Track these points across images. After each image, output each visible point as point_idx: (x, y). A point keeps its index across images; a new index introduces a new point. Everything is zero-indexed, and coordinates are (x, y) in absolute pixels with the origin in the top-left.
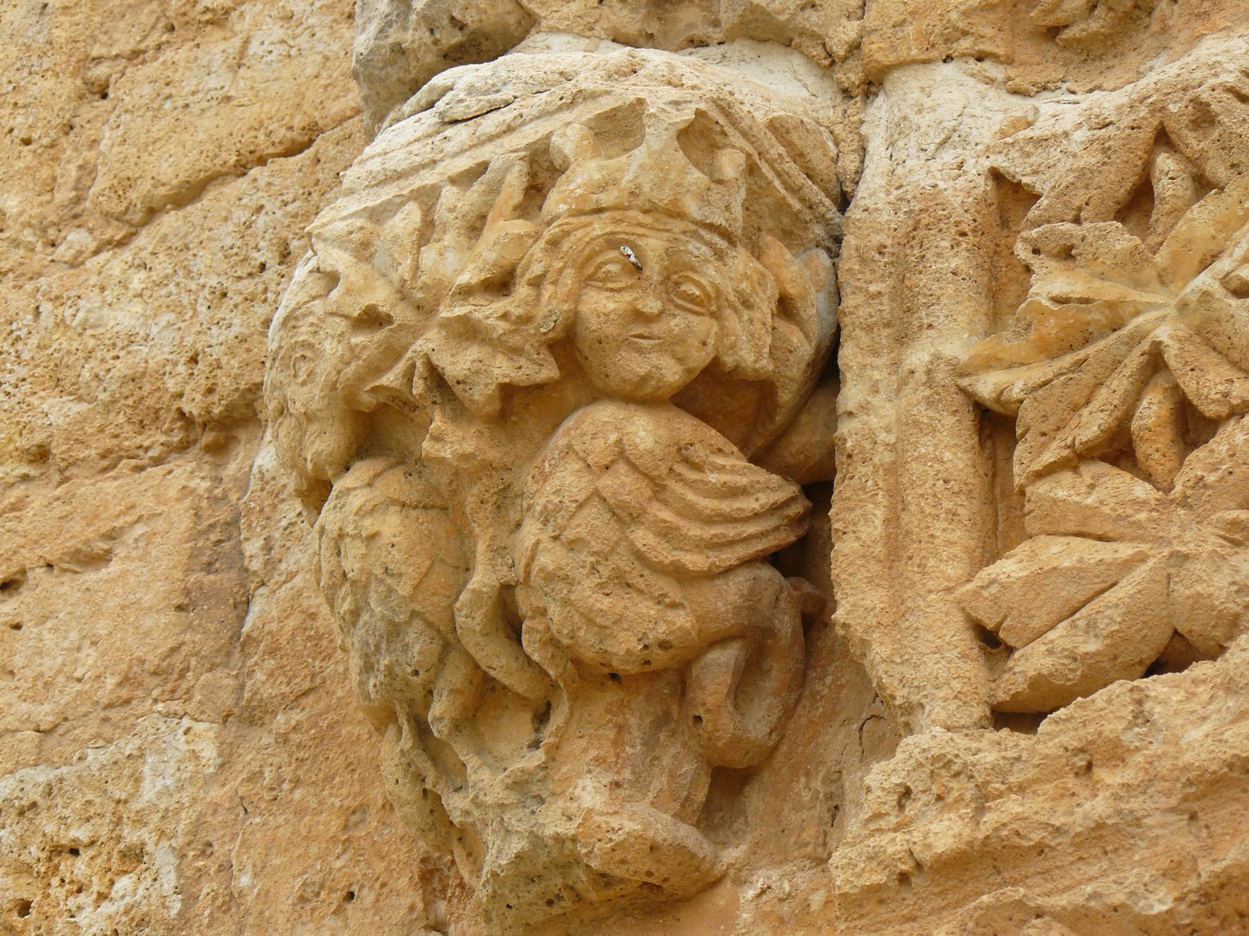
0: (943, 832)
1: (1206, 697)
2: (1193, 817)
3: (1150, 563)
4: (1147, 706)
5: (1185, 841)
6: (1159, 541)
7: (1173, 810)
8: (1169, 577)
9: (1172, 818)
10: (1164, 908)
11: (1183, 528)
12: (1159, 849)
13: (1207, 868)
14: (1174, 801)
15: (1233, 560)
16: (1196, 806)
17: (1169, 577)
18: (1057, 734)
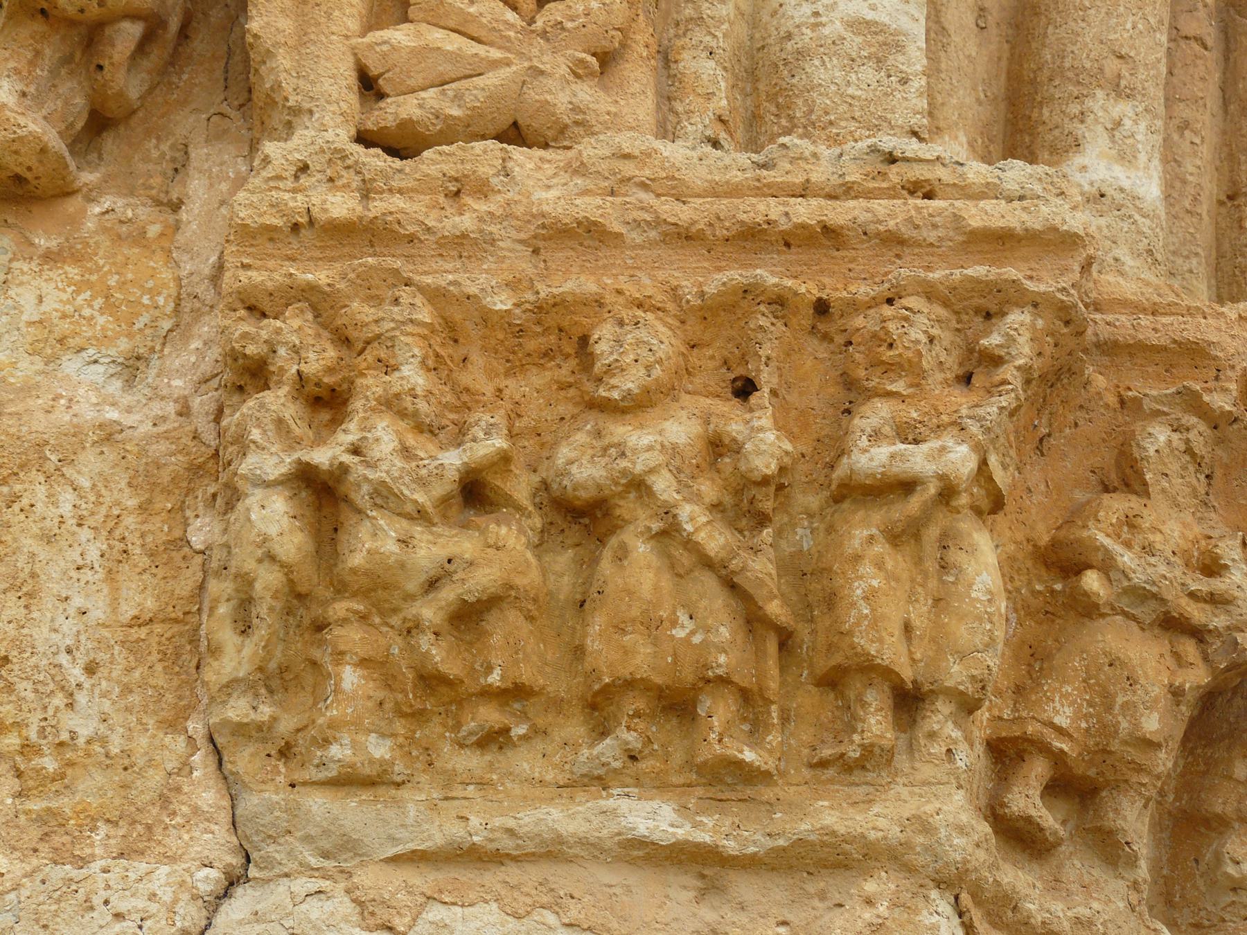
0: (340, 205)
1: (550, 172)
2: (536, 251)
3: (514, 68)
4: (510, 164)
5: (526, 266)
6: (521, 55)
7: (521, 242)
8: (524, 82)
9: (519, 247)
10: (505, 308)
11: (542, 52)
12: (504, 266)
13: (544, 291)
14: (523, 236)
15: (573, 86)
16: (541, 244)
17: (524, 82)
18: (433, 162)
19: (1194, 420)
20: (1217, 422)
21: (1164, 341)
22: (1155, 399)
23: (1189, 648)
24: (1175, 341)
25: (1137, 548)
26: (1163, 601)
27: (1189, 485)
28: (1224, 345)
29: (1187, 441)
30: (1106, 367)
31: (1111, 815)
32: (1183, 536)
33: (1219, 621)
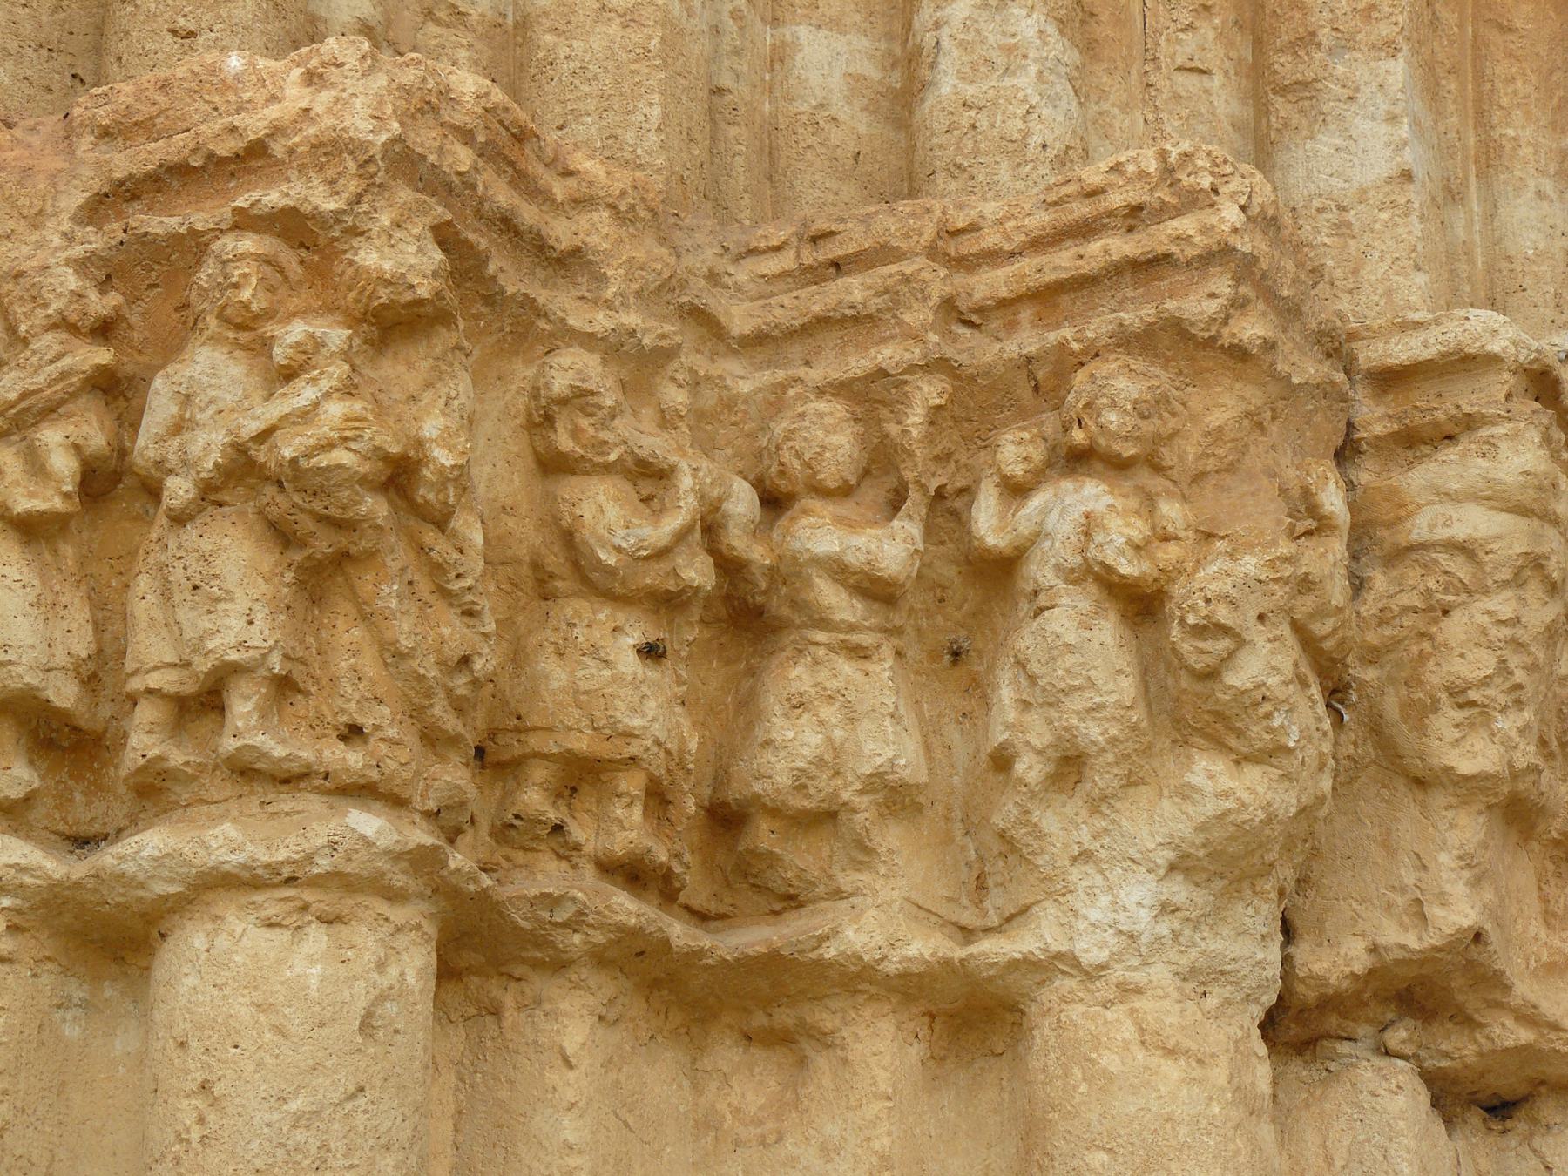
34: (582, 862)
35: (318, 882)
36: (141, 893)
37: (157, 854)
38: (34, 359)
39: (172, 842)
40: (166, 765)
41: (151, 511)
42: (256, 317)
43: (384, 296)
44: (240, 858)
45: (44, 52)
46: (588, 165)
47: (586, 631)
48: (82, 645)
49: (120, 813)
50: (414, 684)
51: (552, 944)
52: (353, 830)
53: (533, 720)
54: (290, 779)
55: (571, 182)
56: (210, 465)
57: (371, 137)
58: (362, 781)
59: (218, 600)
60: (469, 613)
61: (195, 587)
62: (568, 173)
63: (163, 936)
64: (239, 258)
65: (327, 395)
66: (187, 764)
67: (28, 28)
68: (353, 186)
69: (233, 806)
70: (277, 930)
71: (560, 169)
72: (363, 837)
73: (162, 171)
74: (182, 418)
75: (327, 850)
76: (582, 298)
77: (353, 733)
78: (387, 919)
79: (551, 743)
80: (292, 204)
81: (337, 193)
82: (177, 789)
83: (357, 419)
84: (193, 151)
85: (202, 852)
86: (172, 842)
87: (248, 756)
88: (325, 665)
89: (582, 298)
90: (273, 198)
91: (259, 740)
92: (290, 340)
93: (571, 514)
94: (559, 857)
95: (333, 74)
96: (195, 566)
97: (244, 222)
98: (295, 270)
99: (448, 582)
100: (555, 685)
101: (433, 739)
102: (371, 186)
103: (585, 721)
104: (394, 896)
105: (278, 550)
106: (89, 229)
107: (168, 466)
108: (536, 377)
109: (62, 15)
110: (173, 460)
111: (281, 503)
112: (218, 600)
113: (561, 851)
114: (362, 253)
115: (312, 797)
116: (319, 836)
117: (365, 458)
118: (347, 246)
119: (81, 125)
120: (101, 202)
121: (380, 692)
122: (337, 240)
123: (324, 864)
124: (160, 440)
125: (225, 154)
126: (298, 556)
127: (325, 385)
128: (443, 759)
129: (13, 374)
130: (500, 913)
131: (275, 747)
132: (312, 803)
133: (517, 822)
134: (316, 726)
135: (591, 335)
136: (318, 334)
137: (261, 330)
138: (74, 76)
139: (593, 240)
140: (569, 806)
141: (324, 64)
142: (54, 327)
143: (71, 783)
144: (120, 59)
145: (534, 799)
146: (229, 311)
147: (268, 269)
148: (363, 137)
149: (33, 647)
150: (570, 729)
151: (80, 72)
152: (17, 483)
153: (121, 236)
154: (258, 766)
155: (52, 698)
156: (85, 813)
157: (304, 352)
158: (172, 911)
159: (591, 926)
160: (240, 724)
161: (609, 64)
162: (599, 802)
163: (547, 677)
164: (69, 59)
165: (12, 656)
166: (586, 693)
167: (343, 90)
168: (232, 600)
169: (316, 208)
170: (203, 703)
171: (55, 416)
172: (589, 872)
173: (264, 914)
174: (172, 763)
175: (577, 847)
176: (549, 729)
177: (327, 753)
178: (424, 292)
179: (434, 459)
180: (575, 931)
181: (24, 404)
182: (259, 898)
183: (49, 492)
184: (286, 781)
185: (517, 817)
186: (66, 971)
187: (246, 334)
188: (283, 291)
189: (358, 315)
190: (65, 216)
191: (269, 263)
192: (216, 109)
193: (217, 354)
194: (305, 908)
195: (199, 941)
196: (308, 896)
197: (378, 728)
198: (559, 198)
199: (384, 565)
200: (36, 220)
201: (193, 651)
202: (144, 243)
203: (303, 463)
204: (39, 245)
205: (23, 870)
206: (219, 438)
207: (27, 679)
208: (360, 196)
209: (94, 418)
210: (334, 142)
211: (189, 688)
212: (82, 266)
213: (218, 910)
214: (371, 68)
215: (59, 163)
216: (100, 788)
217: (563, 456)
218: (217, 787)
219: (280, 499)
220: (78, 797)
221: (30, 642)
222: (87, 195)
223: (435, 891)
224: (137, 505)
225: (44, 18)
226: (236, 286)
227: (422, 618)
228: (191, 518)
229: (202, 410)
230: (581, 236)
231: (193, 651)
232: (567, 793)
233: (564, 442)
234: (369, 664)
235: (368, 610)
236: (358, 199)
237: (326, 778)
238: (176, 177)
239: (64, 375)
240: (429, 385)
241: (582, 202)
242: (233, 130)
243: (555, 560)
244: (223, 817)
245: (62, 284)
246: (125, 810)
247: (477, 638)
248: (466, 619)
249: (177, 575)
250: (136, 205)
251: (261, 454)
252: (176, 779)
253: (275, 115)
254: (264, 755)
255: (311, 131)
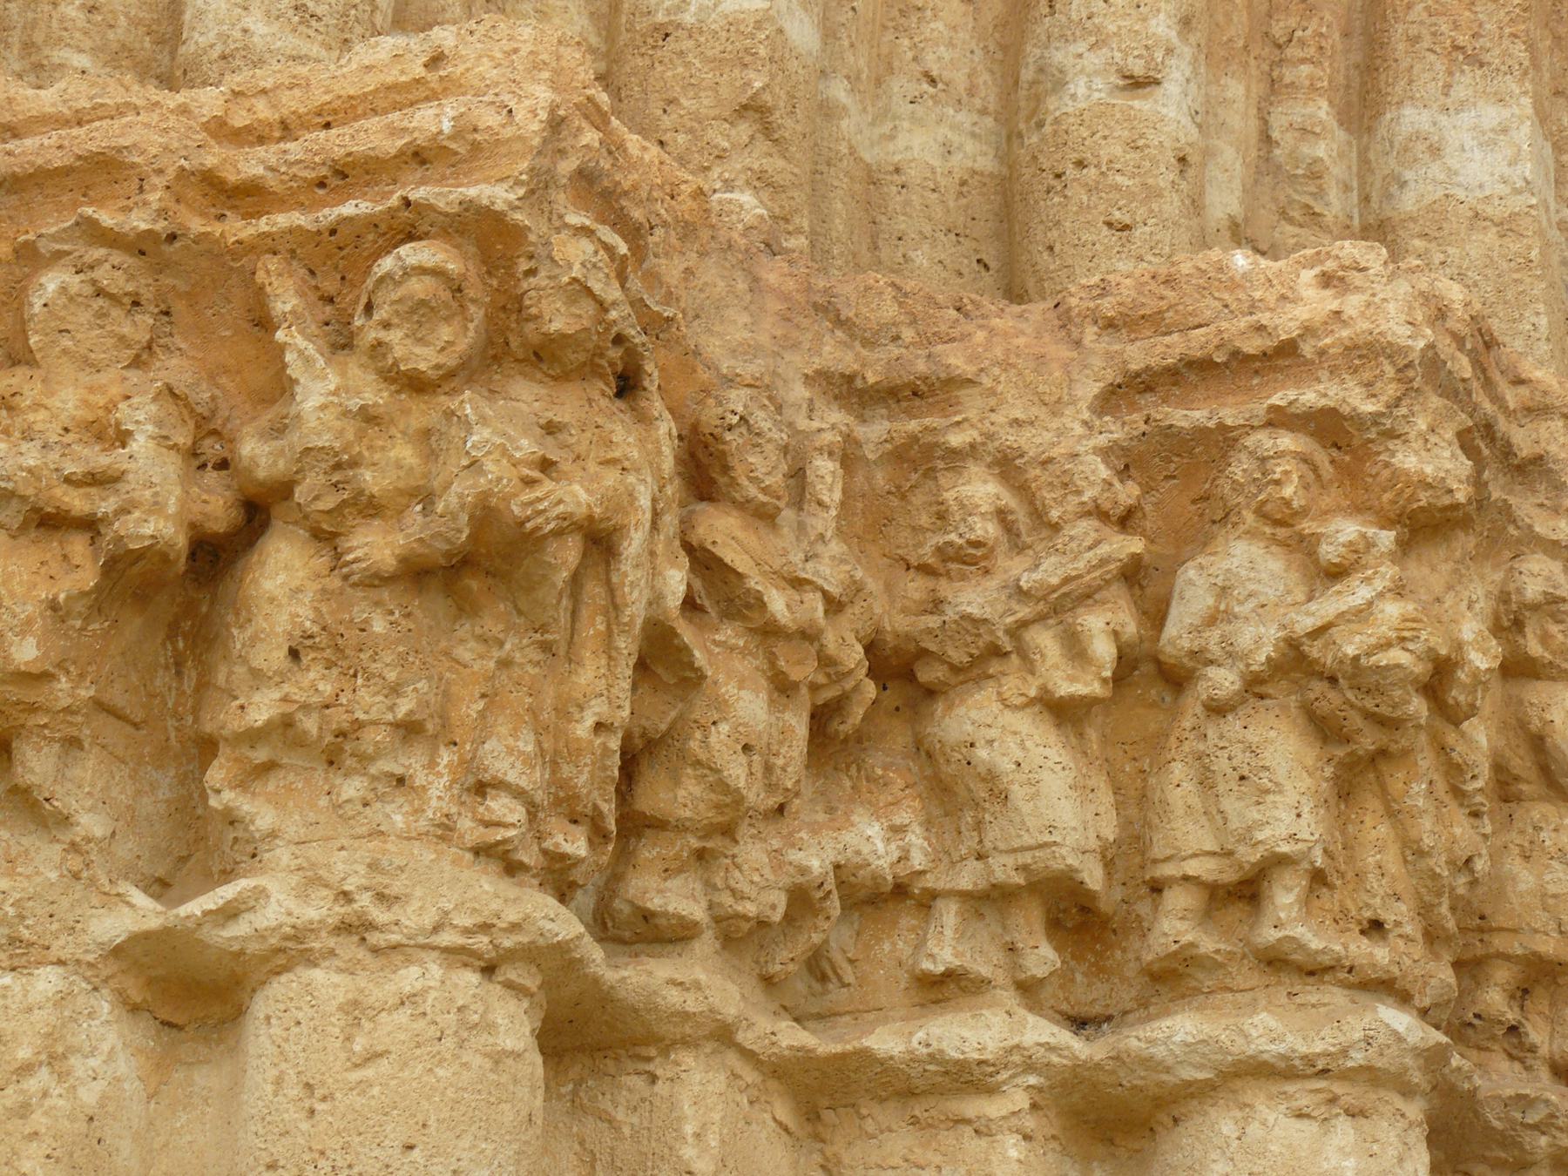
19: (100, 252)
20: (140, 246)
21: (68, 160)
22: (54, 238)
23: (78, 546)
24: (79, 157)
25: (17, 434)
26: (24, 499)
27: (112, 334)
28: (144, 146)
29: (94, 282)
30: (16, 209)
31: (20, 769)
32: (85, 402)
33: (106, 505)
34: (1537, 1064)
35: (1347, 1075)
36: (1165, 1077)
37: (1190, 1039)
38: (1074, 545)
39: (1207, 1028)
40: (1194, 952)
41: (1168, 699)
42: (1296, 514)
43: (1424, 498)
44: (1281, 1048)
45: (952, 236)
46: (1538, 374)
47: (1553, 835)
48: (1110, 830)
49: (1126, 996)
50: (1429, 883)
51: (1520, 1146)
52: (1387, 1025)
53: (1500, 920)
54: (1315, 971)
55: (1523, 391)
56: (1263, 659)
57: (1410, 342)
58: (1385, 977)
59: (1268, 792)
60: (1476, 815)
61: (1242, 778)
62: (1519, 381)
63: (1176, 1120)
64: (1279, 455)
65: (1381, 595)
66: (1218, 951)
67: (938, 212)
68: (1392, 390)
69: (1261, 995)
70: (1306, 1122)
71: (1511, 376)
72: (1395, 1033)
73: (1180, 365)
74: (1217, 609)
75: (1363, 1045)
76: (1541, 505)
77: (1375, 927)
78: (1403, 1115)
79: (1516, 944)
80: (1332, 404)
81: (1374, 396)
82: (1200, 976)
83: (1414, 620)
84: (1217, 347)
85: (1240, 1041)
86: (1207, 1028)
87: (1286, 947)
88: (1350, 859)
89: (1541, 505)
90: (1310, 397)
91: (1300, 931)
92: (1342, 539)
93: (1541, 719)
94: (1511, 1057)
95: (1356, 278)
96: (1241, 758)
97: (1279, 419)
98: (1327, 470)
99: (1465, 782)
100: (1522, 887)
101: (1433, 936)
102: (1409, 390)
103: (1553, 925)
104: (1407, 1091)
105: (1318, 745)
106: (1107, 418)
107: (1209, 656)
108: (1505, 582)
109: (964, 201)
110: (1215, 650)
111: (1330, 700)
112: (1268, 792)
113: (1514, 1052)
114: (1400, 456)
115: (1335, 990)
116: (1355, 1028)
117: (1419, 658)
118: (1382, 448)
119: (1079, 315)
120: (1113, 393)
121: (1400, 888)
122: (1372, 441)
123: (1358, 1058)
124: (1196, 630)
125: (1252, 351)
126: (1340, 752)
127: (1379, 585)
128: (1437, 957)
129: (1053, 559)
130: (1476, 1112)
131: (1315, 939)
132: (1337, 997)
133: (1476, 1022)
134: (1341, 918)
135: (1556, 543)
136: (1370, 534)
137: (1298, 528)
138: (979, 261)
139: (1553, 448)
140: (1522, 1008)
141: (1343, 268)
142: (1088, 514)
143: (1073, 963)
144: (1051, 248)
145: (1495, 999)
146: (1269, 507)
147: (1304, 467)
148: (1402, 342)
149: (1075, 829)
150: (1536, 931)
151: (984, 257)
152: (1056, 667)
153: (1143, 427)
154: (1294, 957)
155: (1087, 880)
156: (1089, 995)
157: (1356, 552)
158: (1192, 1096)
159: (1560, 1129)
160: (1282, 915)
161: (1489, 272)
162: (1552, 1005)
163: (1513, 879)
164: (974, 245)
165: (1056, 838)
166: (1555, 896)
167: (1374, 295)
168: (1280, 792)
169: (1354, 409)
170: (1244, 892)
171: (1090, 601)
172: (1544, 1074)
173: (1295, 1104)
174: (1202, 950)
175: (1533, 1049)
176: (1515, 931)
177: (1352, 947)
178: (1461, 497)
179: (1470, 662)
180: (1544, 1133)
181: (1065, 589)
182: (1290, 1088)
183: (1089, 677)
184: (1311, 973)
185: (1477, 1016)
186: (1064, 1151)
187: (1283, 530)
188: (1315, 489)
189: (1393, 516)
190: (1083, 405)
191: (1305, 461)
192: (1226, 306)
193: (1253, 549)
194: (1333, 1100)
195: (1228, 1128)
196: (1338, 1088)
197: (1398, 924)
198: (1512, 406)
199: (1416, 764)
200: (1055, 408)
201: (1238, 841)
202: (1167, 436)
203: (1363, 661)
204: (1060, 433)
205: (1050, 1048)
206: (1272, 633)
207: (1070, 861)
208: (1399, 399)
209: (1122, 602)
210: (1369, 345)
211: (1230, 876)
212: (1105, 453)
213: (1247, 1098)
214: (1393, 273)
215: (1066, 352)
216: (1101, 970)
217: (1532, 661)
218: (1245, 976)
219: (1332, 695)
220: (1079, 977)
221: (1073, 824)
222: (1102, 384)
223: (1434, 1088)
224: (1153, 692)
225: (951, 204)
226: (1277, 483)
227: (1438, 818)
228: (1233, 709)
229: (1240, 603)
230: (1543, 444)
231: (1238, 841)
232: (1519, 994)
233: (1534, 648)
234: (1391, 859)
235: (1396, 807)
236: (1397, 402)
237: (1350, 972)
238: (1198, 372)
239: (1103, 562)
240: (1450, 588)
241: (1537, 411)
242: (1260, 328)
243: (1522, 763)
244: (1253, 1007)
245: (1093, 472)
246: (1134, 993)
247: (1479, 838)
248: (1472, 820)
249: (1221, 764)
250: (1150, 398)
251: (1314, 650)
252: (1202, 966)
253: (1306, 316)
254: (1302, 947)
255: (1345, 333)
